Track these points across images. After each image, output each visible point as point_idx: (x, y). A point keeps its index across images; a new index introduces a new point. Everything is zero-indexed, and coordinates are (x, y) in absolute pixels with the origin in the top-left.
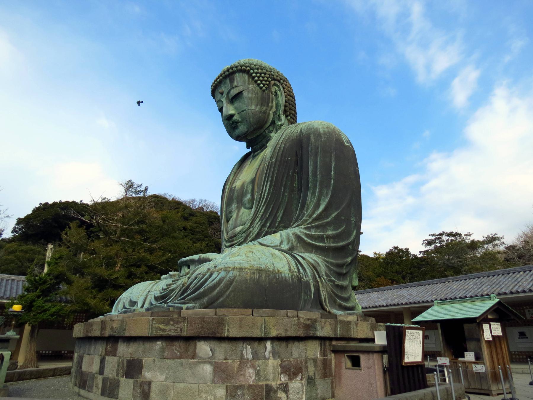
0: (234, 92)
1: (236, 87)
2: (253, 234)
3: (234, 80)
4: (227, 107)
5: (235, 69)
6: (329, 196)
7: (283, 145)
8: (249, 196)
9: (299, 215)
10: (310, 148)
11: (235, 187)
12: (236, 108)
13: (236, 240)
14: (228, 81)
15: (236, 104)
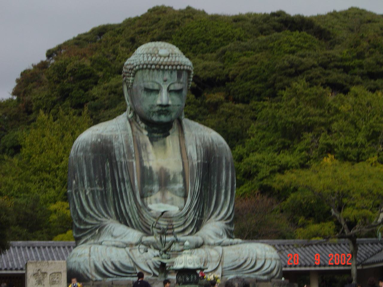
0: (178, 86)
1: (181, 83)
2: (189, 220)
3: (181, 76)
4: (168, 96)
5: (185, 67)
6: (234, 202)
7: (202, 149)
8: (180, 185)
9: (213, 210)
10: (224, 161)
11: (151, 168)
12: (172, 100)
13: (176, 221)
14: (175, 74)
15: (175, 97)
